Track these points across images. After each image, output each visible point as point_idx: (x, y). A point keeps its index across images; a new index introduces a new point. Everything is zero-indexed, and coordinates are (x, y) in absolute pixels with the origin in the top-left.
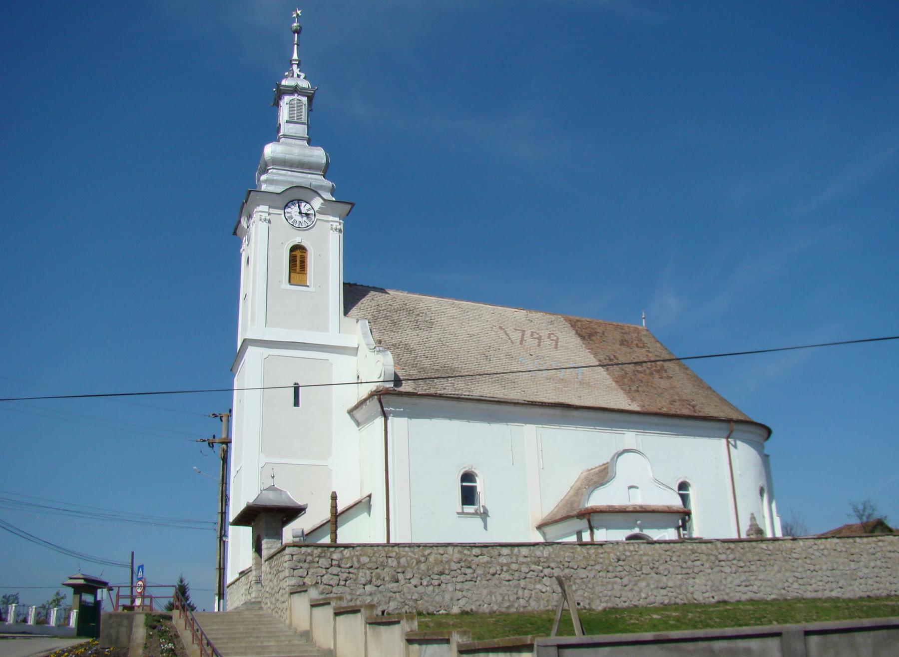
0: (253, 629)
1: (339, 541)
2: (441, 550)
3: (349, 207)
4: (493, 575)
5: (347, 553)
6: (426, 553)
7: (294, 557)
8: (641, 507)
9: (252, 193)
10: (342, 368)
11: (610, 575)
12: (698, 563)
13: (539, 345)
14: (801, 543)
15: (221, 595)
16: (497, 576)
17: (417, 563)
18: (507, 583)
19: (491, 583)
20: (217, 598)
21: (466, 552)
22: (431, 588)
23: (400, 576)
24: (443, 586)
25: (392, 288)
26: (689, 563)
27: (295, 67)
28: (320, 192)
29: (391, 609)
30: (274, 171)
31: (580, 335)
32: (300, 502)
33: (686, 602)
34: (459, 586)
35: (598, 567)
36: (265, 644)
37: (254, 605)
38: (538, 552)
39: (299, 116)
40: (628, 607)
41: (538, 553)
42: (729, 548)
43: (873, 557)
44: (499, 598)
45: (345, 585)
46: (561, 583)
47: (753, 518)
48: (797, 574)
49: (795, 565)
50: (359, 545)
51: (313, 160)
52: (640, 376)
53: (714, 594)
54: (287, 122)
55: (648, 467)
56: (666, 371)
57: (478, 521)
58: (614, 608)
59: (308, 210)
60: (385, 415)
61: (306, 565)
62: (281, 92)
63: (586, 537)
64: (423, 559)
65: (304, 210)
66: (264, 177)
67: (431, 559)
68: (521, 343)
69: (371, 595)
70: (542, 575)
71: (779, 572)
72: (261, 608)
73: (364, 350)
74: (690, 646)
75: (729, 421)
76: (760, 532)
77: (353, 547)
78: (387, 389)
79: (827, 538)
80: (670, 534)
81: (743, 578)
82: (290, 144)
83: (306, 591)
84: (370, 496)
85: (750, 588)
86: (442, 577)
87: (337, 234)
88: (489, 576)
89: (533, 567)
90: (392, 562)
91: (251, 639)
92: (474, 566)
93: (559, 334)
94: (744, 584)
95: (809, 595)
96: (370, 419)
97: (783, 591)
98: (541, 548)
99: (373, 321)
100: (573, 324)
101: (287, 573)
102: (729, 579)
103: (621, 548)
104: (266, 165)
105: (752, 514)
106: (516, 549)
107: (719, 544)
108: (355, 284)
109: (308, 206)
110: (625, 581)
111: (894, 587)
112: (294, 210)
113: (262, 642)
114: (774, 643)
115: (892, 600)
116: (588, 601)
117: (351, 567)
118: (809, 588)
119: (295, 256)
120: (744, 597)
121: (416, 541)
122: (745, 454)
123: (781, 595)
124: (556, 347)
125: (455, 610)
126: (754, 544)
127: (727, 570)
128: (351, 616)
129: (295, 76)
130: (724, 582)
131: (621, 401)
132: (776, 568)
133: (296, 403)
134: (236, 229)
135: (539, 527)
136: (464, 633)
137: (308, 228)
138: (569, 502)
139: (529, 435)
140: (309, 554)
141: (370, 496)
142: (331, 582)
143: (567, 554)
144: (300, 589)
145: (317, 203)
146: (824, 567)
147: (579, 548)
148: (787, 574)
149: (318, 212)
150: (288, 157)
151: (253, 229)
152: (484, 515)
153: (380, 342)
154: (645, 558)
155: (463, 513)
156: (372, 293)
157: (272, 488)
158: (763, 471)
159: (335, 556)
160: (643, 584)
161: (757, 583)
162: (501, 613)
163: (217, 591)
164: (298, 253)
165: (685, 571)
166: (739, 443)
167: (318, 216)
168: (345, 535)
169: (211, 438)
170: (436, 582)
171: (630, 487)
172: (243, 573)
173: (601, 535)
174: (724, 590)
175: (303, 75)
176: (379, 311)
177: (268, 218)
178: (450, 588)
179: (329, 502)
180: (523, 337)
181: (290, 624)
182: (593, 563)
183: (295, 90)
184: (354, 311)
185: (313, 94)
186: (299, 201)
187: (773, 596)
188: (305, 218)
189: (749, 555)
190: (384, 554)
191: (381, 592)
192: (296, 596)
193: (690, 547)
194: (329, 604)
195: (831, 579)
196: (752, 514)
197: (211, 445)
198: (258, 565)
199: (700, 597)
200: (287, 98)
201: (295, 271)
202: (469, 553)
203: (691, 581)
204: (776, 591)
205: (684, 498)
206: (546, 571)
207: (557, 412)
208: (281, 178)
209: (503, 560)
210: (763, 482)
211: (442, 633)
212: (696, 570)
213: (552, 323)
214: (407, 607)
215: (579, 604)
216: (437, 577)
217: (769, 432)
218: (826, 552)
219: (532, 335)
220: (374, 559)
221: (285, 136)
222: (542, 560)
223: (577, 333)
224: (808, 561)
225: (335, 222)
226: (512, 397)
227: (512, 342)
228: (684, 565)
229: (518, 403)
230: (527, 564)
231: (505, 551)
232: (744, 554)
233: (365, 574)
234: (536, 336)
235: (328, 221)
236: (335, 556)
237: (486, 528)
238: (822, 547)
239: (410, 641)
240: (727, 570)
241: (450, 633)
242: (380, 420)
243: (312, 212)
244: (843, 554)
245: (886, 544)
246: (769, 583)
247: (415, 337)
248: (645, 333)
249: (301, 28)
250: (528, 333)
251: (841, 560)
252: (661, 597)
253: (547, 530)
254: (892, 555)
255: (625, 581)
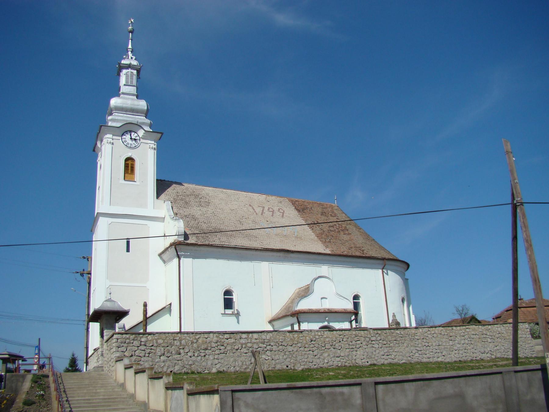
0: (94, 382)
1: (149, 330)
2: (206, 336)
3: (160, 135)
4: (237, 350)
5: (150, 337)
6: (197, 337)
7: (119, 340)
8: (328, 309)
9: (103, 127)
10: (156, 228)
11: (306, 349)
12: (358, 342)
13: (272, 216)
14: (421, 330)
15: (87, 363)
16: (239, 350)
17: (192, 343)
18: (245, 355)
19: (236, 354)
20: (85, 365)
21: (220, 336)
22: (200, 358)
23: (182, 351)
24: (207, 356)
25: (186, 183)
26: (354, 342)
27: (130, 53)
28: (143, 126)
29: (175, 370)
30: (116, 114)
31: (297, 210)
32: (126, 308)
33: (351, 365)
34: (216, 357)
35: (299, 345)
36: (98, 391)
37: (100, 368)
38: (263, 336)
39: (132, 82)
40: (317, 368)
41: (264, 337)
42: (377, 333)
43: (463, 338)
44: (240, 364)
45: (148, 356)
46: (254, 354)
47: (394, 316)
48: (418, 348)
49: (417, 343)
50: (157, 333)
51: (140, 107)
52: (332, 233)
53: (368, 360)
54: (125, 85)
55: (334, 286)
56: (347, 230)
57: (234, 318)
58: (308, 369)
59: (136, 137)
60: (179, 257)
61: (126, 345)
62: (121, 68)
63: (296, 327)
64: (195, 341)
65: (133, 137)
66: (110, 118)
67: (200, 341)
68: (262, 214)
69: (164, 362)
70: (266, 349)
71: (407, 347)
72: (103, 370)
73: (168, 219)
74: (308, 391)
75: (383, 259)
76: (398, 323)
77: (154, 334)
78: (180, 242)
79: (436, 327)
80: (346, 325)
81: (386, 350)
82: (126, 98)
83: (122, 360)
84: (170, 304)
85: (390, 357)
86: (206, 351)
87: (153, 151)
88: (234, 351)
89: (261, 345)
90: (177, 343)
91: (91, 388)
92: (225, 345)
93: (284, 209)
94: (386, 354)
95: (425, 360)
96: (171, 259)
97: (409, 358)
98: (266, 334)
99: (174, 202)
100: (294, 203)
101: (114, 349)
102: (377, 351)
103: (313, 334)
104: (112, 111)
105: (394, 313)
106: (251, 335)
107: (371, 331)
108: (164, 180)
109: (136, 135)
110: (315, 353)
111: (475, 355)
112: (127, 137)
113: (96, 390)
114: (357, 389)
115: (473, 363)
116: (293, 365)
117: (153, 346)
118: (424, 356)
119: (128, 164)
120: (386, 362)
121: (196, 330)
122: (393, 279)
123: (408, 360)
124: (283, 216)
125: (214, 370)
126: (392, 331)
127: (376, 346)
128: (142, 374)
129: (130, 58)
130: (374, 353)
131: (319, 248)
132: (405, 345)
133: (128, 250)
134: (94, 148)
135: (270, 322)
136: (191, 383)
137: (135, 147)
138: (288, 307)
139: (264, 268)
140: (127, 339)
141: (170, 304)
142: (140, 355)
143: (281, 337)
144: (119, 360)
145: (141, 133)
146: (434, 344)
147: (288, 334)
148: (412, 348)
149: (141, 138)
150: (124, 106)
151: (103, 148)
152: (237, 315)
153: (176, 214)
154: (327, 340)
155: (225, 314)
156: (174, 185)
157: (109, 300)
158: (404, 288)
159: (143, 340)
160: (326, 355)
161: (394, 354)
162: (241, 372)
163: (85, 361)
164: (130, 162)
165: (351, 347)
166: (389, 272)
167: (142, 140)
168: (151, 328)
169: (82, 271)
170: (203, 354)
171: (322, 298)
172: (95, 350)
173: (305, 326)
174: (374, 358)
175: (134, 58)
176: (178, 196)
177: (112, 142)
178: (211, 357)
179: (142, 308)
180: (263, 211)
181: (116, 380)
182: (296, 343)
183: (129, 66)
184: (163, 196)
185: (140, 69)
186: (131, 131)
187: (403, 361)
188: (134, 142)
189: (390, 337)
190: (172, 338)
191: (170, 360)
192: (118, 363)
193: (354, 333)
194: (132, 367)
195: (438, 351)
196: (394, 313)
197: (82, 275)
198: (102, 345)
199: (359, 362)
200: (124, 71)
201: (128, 173)
202: (222, 337)
203: (354, 353)
204: (405, 358)
205: (356, 305)
206: (268, 347)
207: (281, 254)
208: (119, 118)
209: (243, 341)
210: (404, 295)
211: (180, 384)
212: (358, 346)
213: (281, 202)
214: (185, 369)
215: (287, 366)
216: (203, 351)
217: (408, 266)
218: (435, 335)
219: (269, 209)
220: (166, 341)
221: (123, 93)
222: (266, 341)
223: (295, 208)
224: (425, 340)
225: (152, 144)
226: (254, 246)
227: (257, 214)
228: (351, 344)
229: (257, 249)
230: (257, 343)
231: (244, 336)
232: (387, 337)
233: (161, 350)
234: (271, 210)
235: (147, 143)
236: (143, 340)
237: (238, 322)
238: (433, 332)
239: (167, 388)
240: (376, 346)
241: (183, 384)
242: (176, 260)
243: (138, 138)
244: (445, 336)
245: (471, 330)
246: (401, 354)
247: (199, 211)
248: (336, 208)
249: (133, 30)
250: (266, 208)
251: (444, 340)
252: (337, 362)
253: (275, 323)
254: (475, 336)
255: (315, 353)
